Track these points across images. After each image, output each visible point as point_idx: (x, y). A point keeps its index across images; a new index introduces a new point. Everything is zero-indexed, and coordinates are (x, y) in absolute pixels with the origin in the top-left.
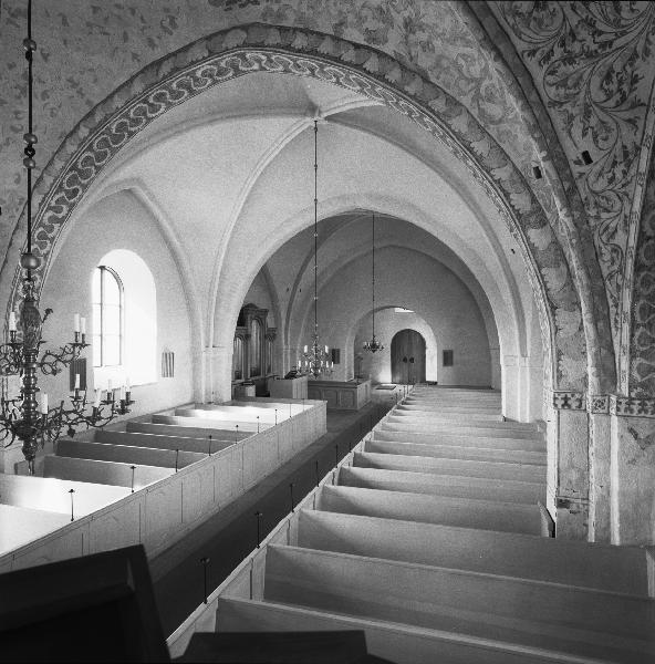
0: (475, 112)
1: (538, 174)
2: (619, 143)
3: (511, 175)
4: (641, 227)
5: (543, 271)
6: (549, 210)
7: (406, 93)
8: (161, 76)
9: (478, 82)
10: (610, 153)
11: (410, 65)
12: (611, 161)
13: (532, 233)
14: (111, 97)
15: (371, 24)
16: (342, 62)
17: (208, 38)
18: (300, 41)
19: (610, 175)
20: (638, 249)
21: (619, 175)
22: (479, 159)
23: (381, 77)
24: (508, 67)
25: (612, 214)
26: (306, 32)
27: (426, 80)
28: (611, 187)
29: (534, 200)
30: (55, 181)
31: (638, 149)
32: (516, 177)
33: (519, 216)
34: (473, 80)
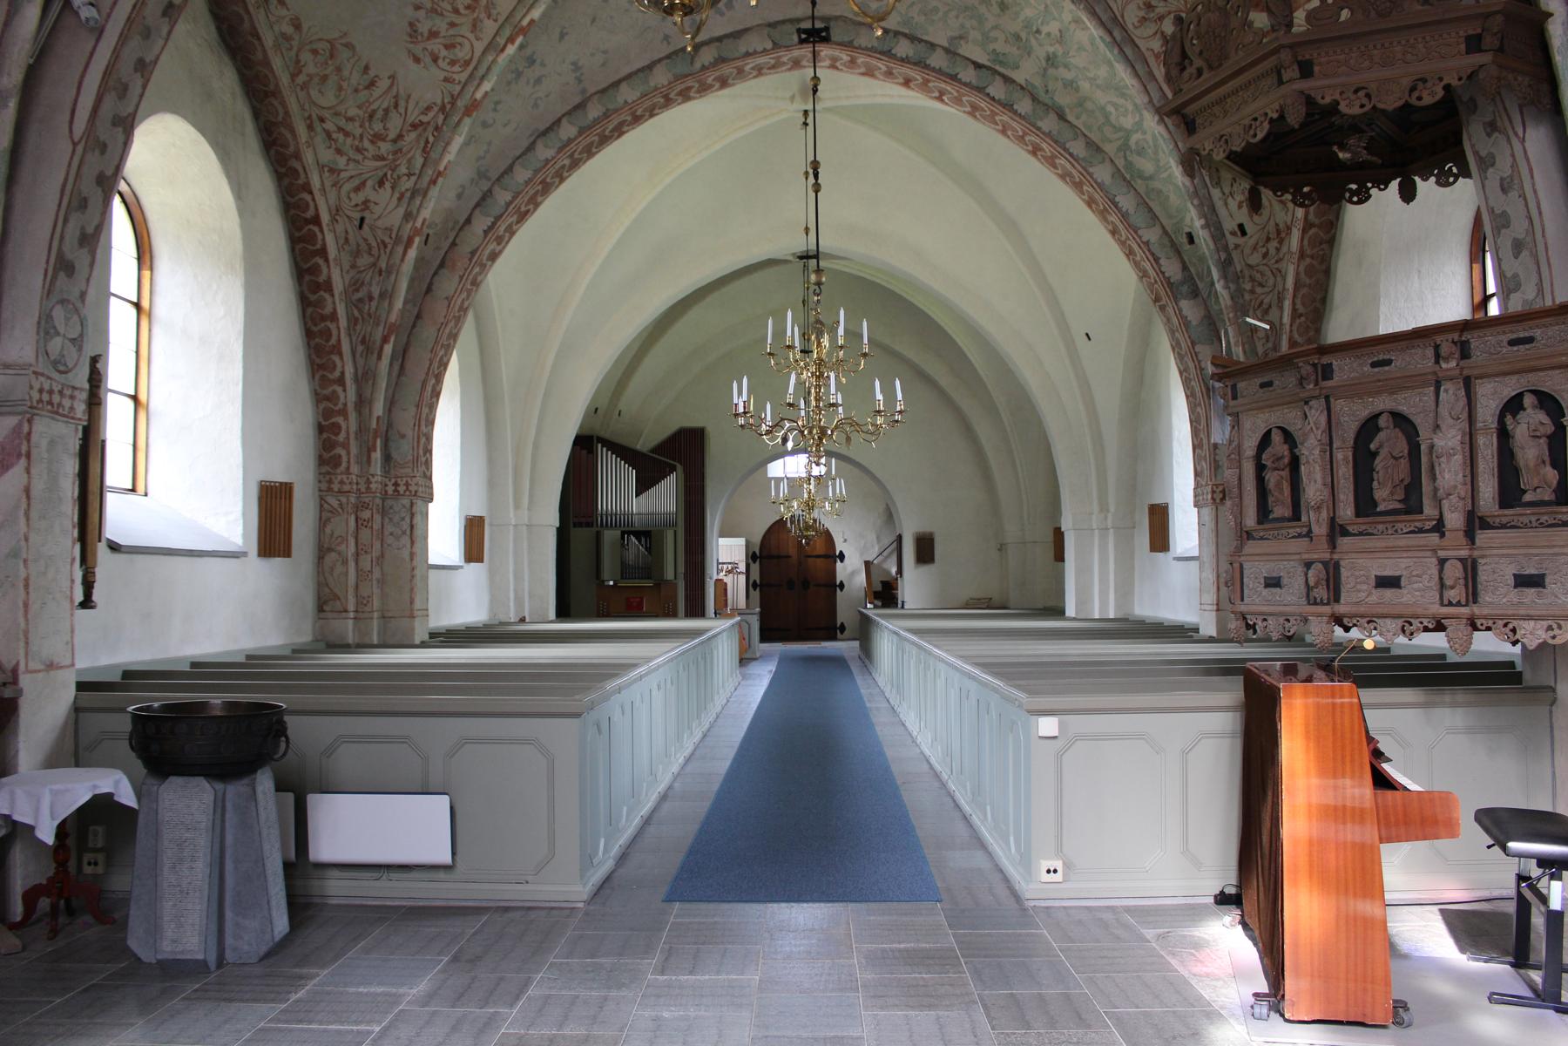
0: (1120, 163)
1: (1191, 238)
2: (1272, 223)
3: (1161, 236)
4: (1294, 303)
5: (1198, 348)
6: (1201, 279)
7: (1039, 129)
8: (698, 65)
9: (1128, 133)
10: (1264, 228)
11: (1043, 97)
12: (1264, 236)
13: (1185, 304)
14: (616, 85)
15: (1000, 47)
16: (960, 81)
17: (772, 25)
18: (903, 48)
19: (1264, 250)
20: (1291, 325)
21: (1272, 251)
22: (1124, 216)
23: (1008, 106)
24: (1170, 132)
25: (1266, 289)
26: (913, 39)
27: (1061, 117)
28: (1265, 262)
29: (1185, 268)
30: (514, 198)
31: (1289, 228)
32: (1166, 241)
33: (1170, 285)
34: (1120, 129)
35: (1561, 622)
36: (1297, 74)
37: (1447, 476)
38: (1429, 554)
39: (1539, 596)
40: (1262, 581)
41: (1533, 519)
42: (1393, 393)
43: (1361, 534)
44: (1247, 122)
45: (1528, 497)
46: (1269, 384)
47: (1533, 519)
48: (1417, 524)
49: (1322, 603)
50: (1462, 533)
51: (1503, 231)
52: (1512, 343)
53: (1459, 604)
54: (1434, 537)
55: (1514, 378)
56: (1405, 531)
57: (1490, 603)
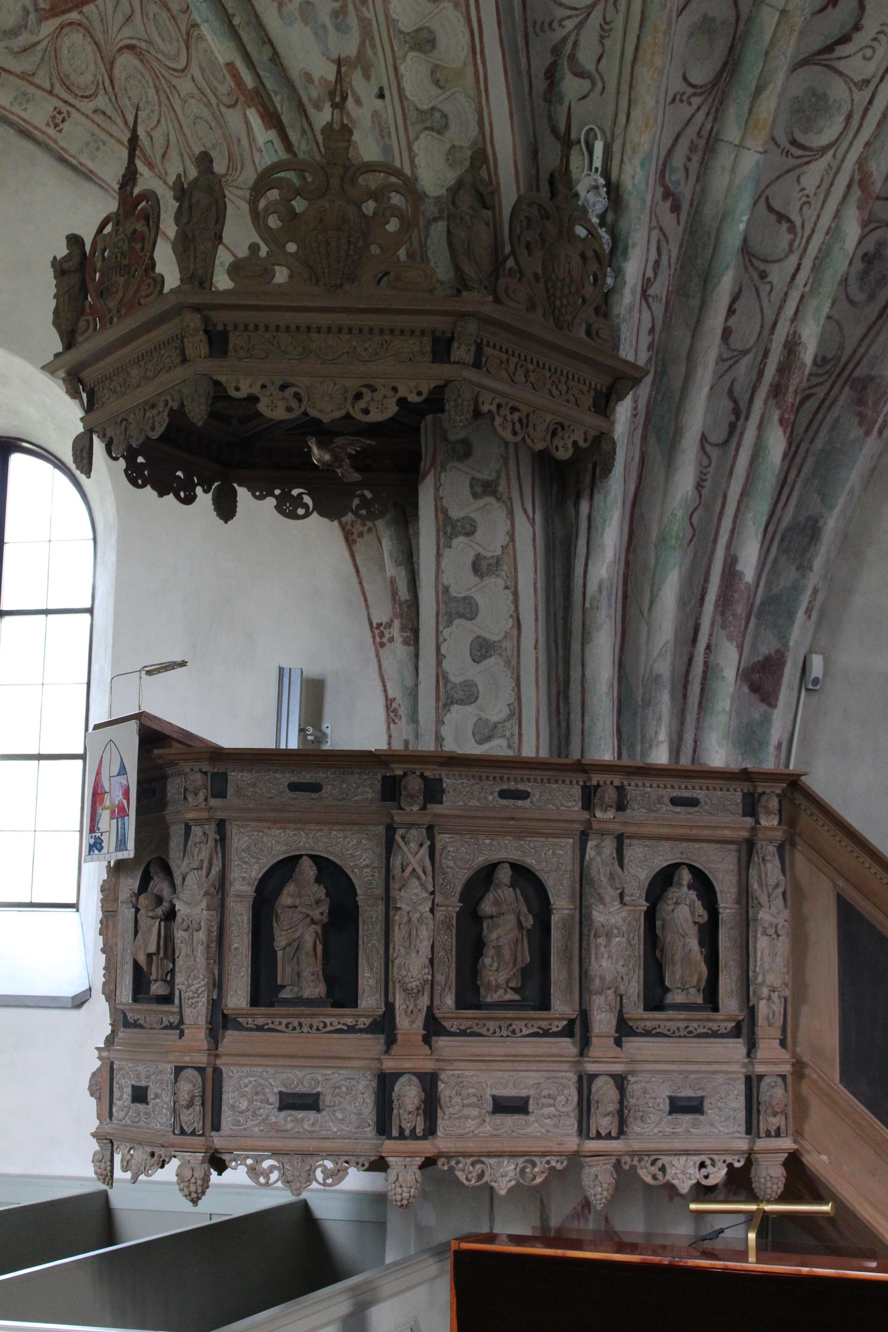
35: (715, 1157)
36: (470, 358)
37: (604, 963)
38: (566, 1066)
39: (695, 1125)
40: (274, 1099)
41: (682, 1025)
42: (520, 838)
43: (463, 1033)
44: (352, 385)
45: (670, 999)
46: (315, 788)
47: (682, 1025)
48: (544, 1024)
49: (413, 1136)
50: (612, 1040)
51: (457, 621)
52: (675, 801)
53: (609, 1136)
54: (567, 1046)
55: (667, 845)
56: (525, 1032)
57: (638, 1134)
